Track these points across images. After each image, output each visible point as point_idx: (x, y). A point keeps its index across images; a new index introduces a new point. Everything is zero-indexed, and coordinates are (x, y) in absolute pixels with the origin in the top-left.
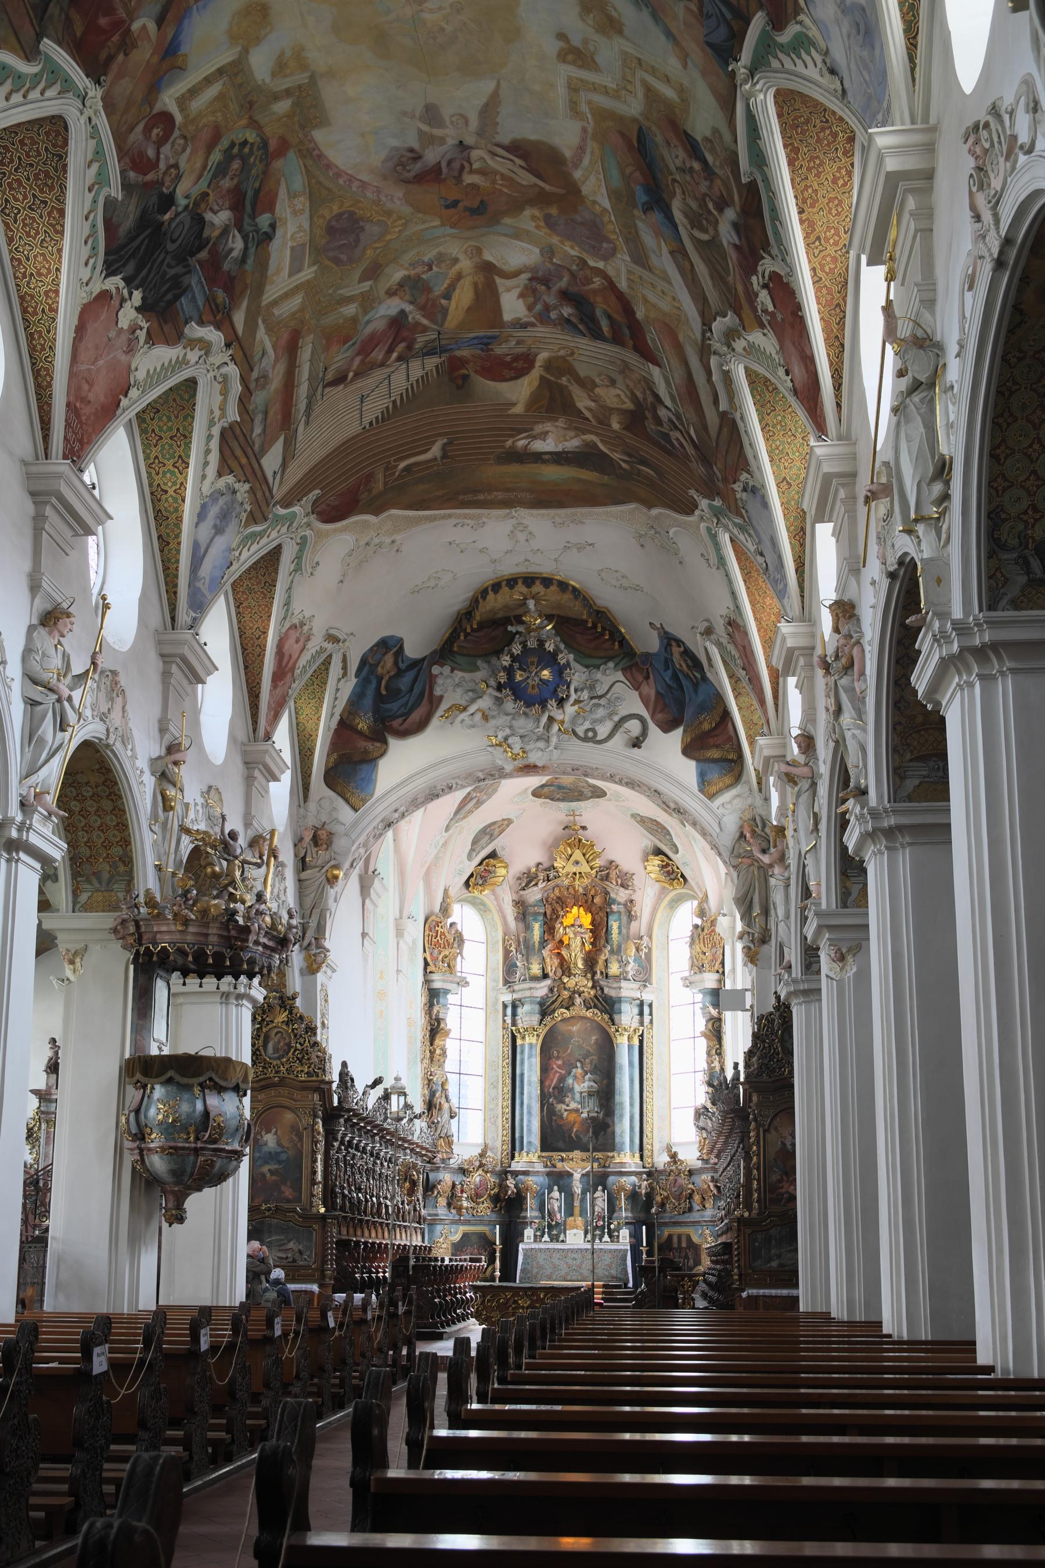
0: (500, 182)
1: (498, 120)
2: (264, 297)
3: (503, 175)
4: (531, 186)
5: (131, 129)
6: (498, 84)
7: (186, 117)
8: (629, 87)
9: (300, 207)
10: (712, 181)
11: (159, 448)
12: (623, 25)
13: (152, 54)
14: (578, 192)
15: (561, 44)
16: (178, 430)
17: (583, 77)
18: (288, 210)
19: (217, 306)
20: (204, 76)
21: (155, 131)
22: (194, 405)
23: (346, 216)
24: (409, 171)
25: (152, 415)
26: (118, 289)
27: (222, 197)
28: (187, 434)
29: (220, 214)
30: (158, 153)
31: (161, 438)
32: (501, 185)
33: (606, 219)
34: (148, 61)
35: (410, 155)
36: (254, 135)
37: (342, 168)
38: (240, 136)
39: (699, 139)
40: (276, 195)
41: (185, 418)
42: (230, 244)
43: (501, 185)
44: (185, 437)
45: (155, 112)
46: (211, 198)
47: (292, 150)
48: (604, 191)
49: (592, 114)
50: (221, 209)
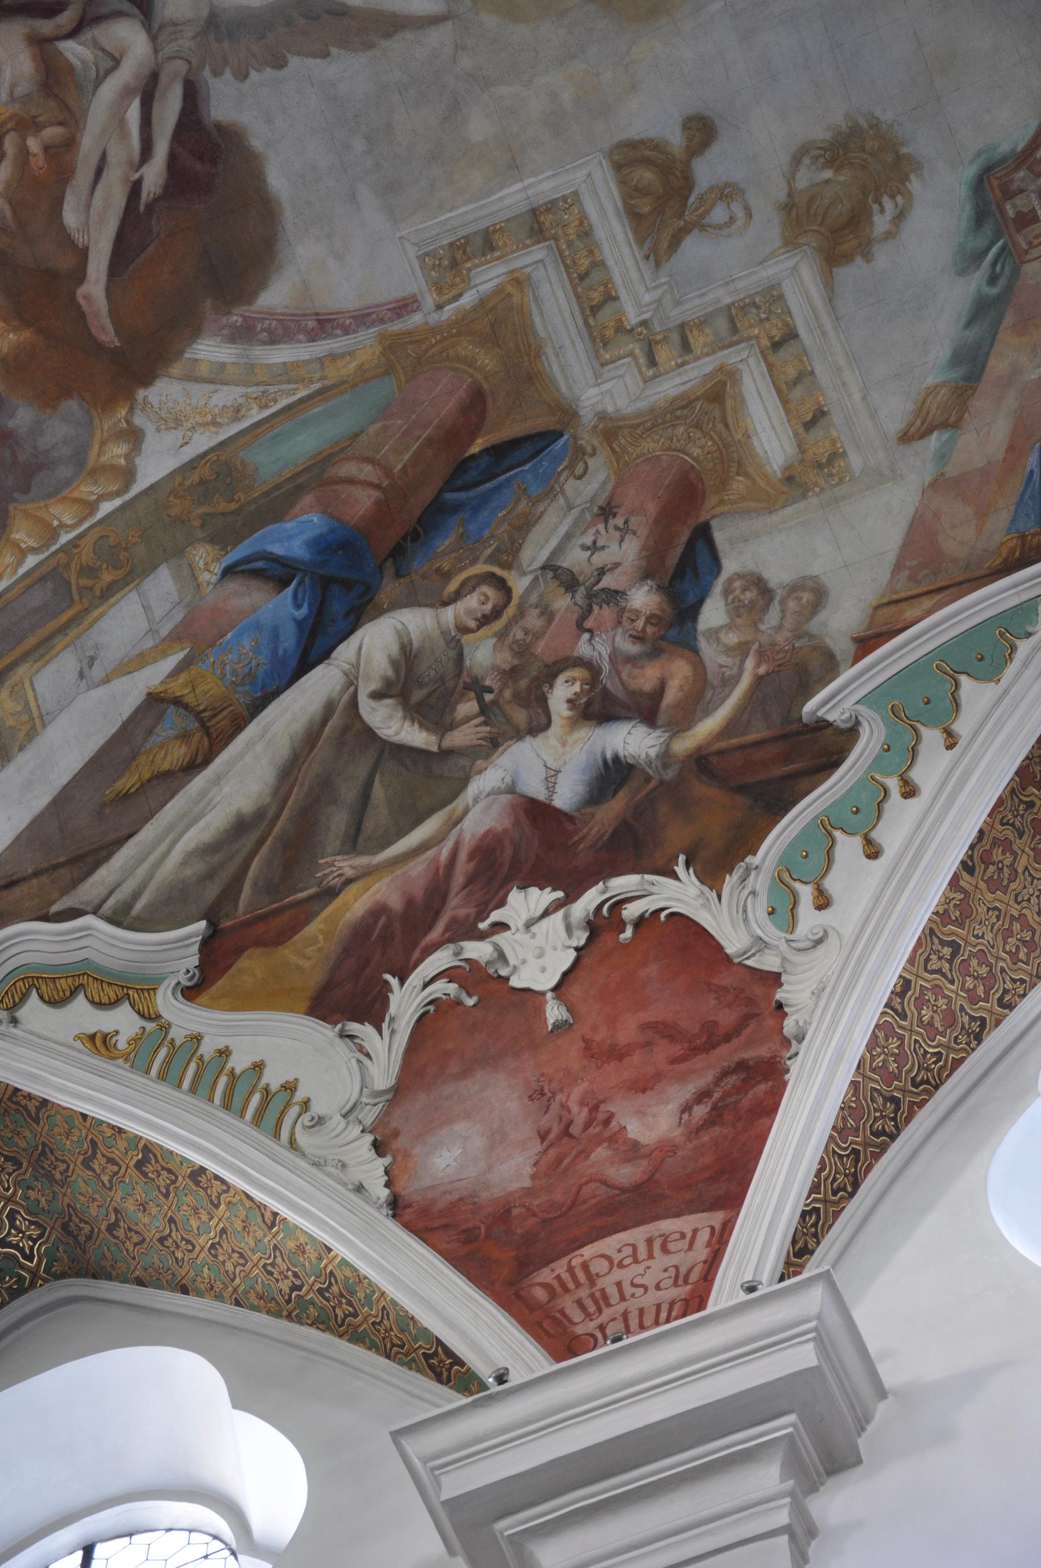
0: (33, 144)
1: (294, 62)
3: (70, 143)
4: (65, 239)
6: (434, 20)
8: (663, 354)
10: (655, 653)
12: (867, 257)
14: (147, 379)
15: (676, 139)
17: (600, 233)
32: (24, 152)
33: (86, 490)
39: (730, 566)
43: (24, 152)
48: (203, 442)
49: (482, 303)
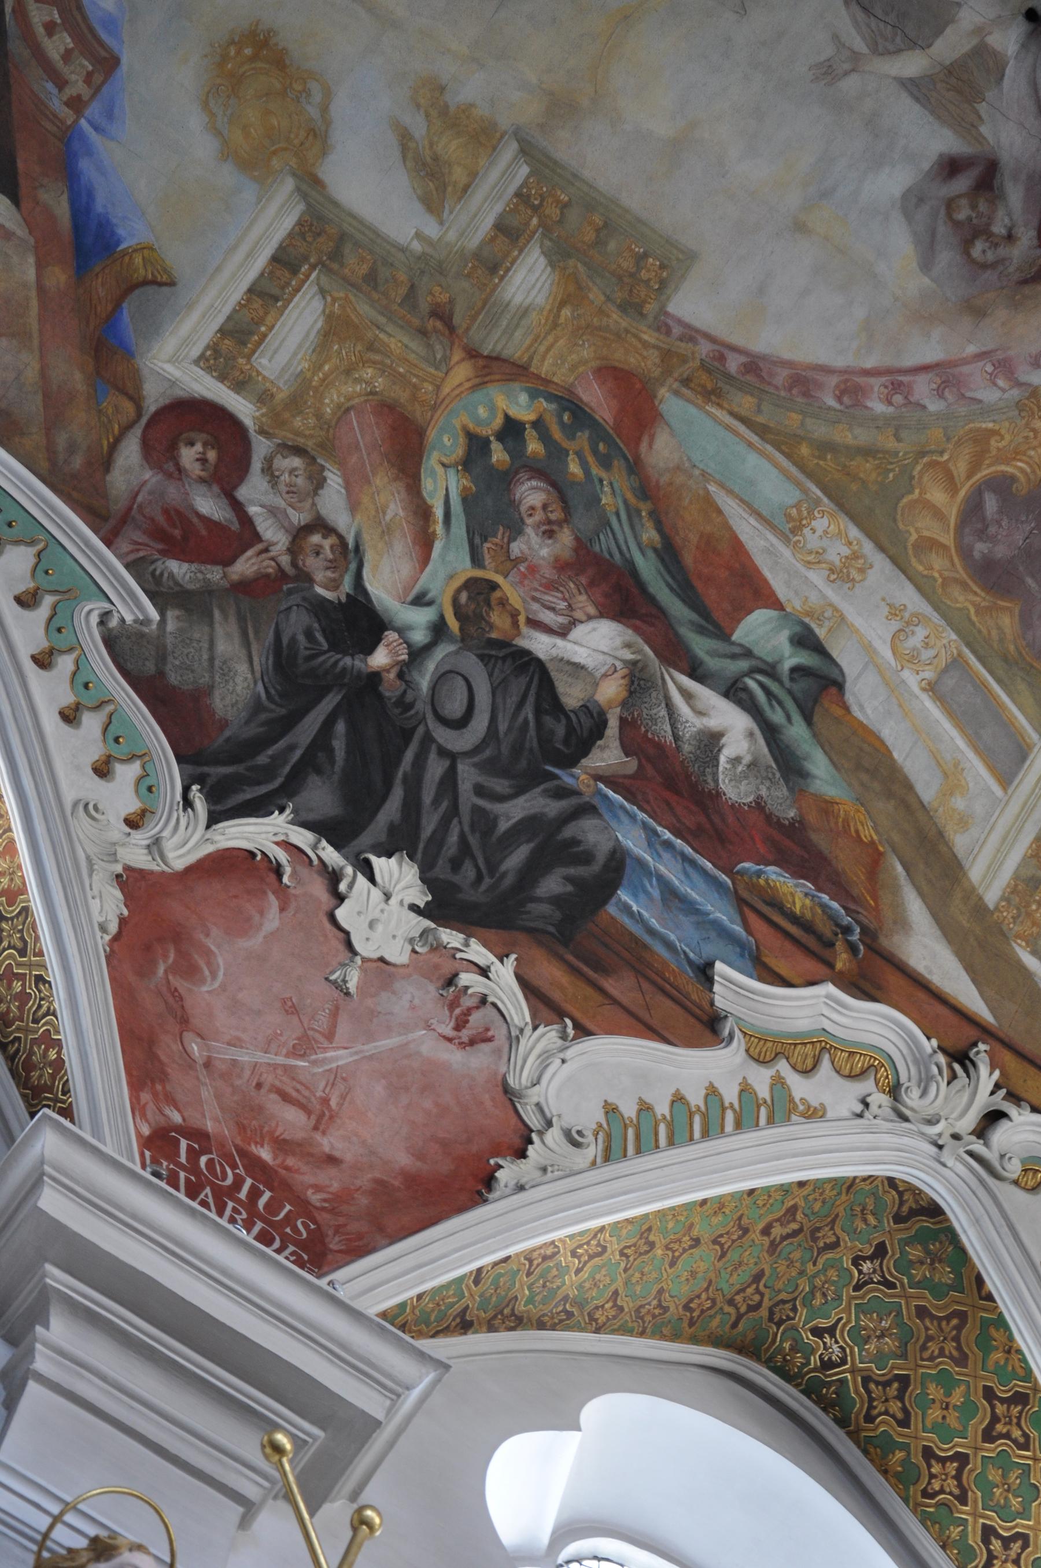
2: (975, 874)
5: (107, 463)
7: (263, 398)
9: (836, 552)
11: (976, 1494)
13: (40, 266)
16: (989, 1394)
18: (817, 577)
19: (807, 926)
20: (244, 286)
21: (188, 455)
22: (980, 1281)
23: (991, 504)
24: (1010, 238)
25: (895, 1407)
26: (287, 845)
27: (550, 586)
28: (1021, 1387)
29: (579, 632)
30: (238, 507)
31: (962, 1459)
34: (41, 289)
35: (962, 184)
36: (523, 398)
37: (840, 363)
38: (482, 412)
40: (738, 547)
41: (985, 1344)
42: (691, 722)
44: (1020, 1399)
45: (151, 406)
46: (510, 589)
47: (663, 392)
50: (574, 623)
